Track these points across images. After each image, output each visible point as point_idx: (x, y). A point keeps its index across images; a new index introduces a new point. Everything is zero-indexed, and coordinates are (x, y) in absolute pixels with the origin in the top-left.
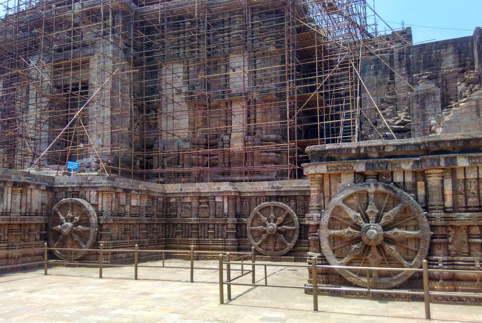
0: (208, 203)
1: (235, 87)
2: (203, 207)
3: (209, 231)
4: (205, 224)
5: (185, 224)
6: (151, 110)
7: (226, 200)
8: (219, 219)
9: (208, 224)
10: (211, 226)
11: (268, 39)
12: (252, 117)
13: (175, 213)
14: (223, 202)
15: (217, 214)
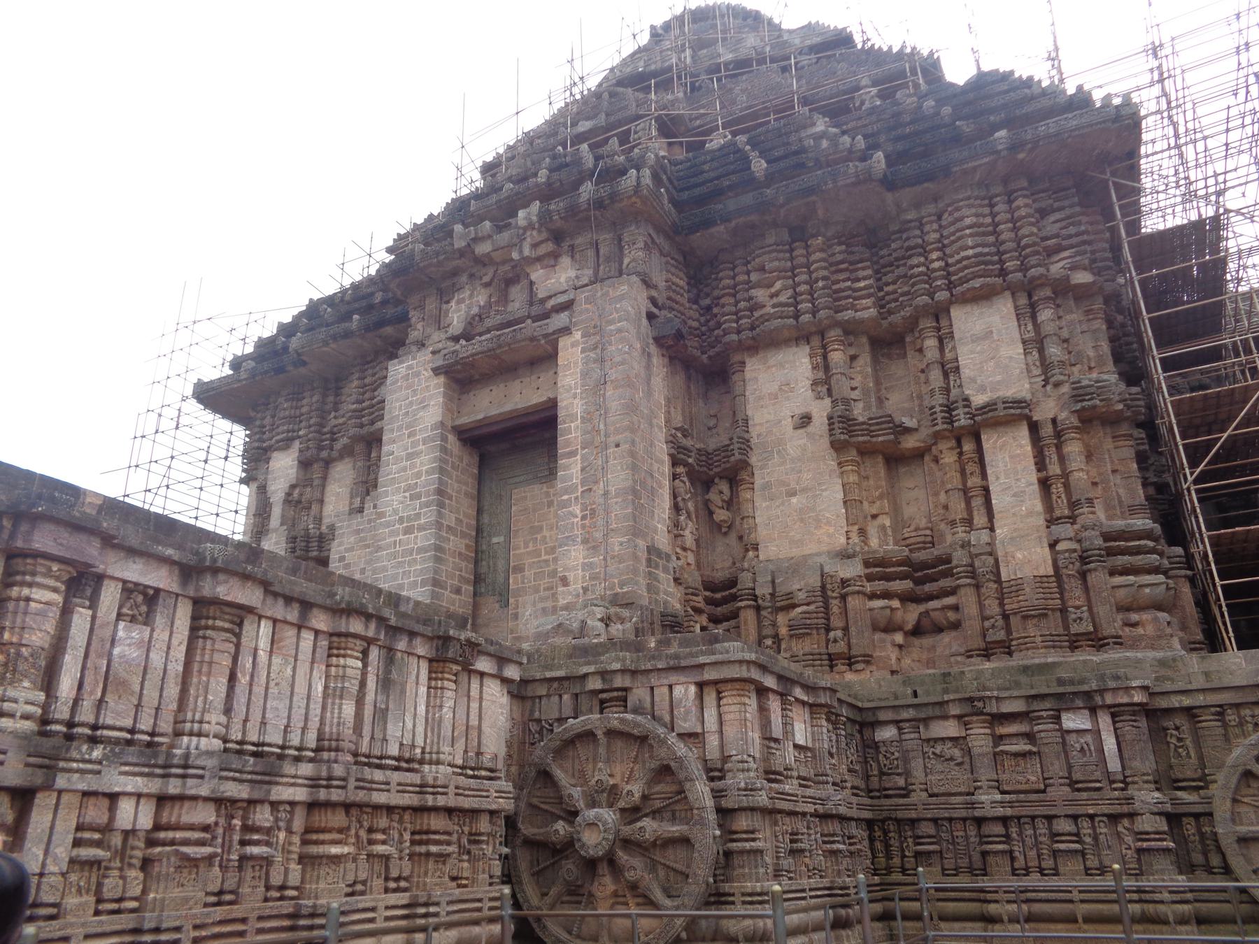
0: (1030, 737)
1: (982, 389)
2: (1016, 755)
3: (1062, 846)
4: (1033, 818)
5: (950, 820)
6: (717, 480)
7: (1105, 721)
8: (1095, 795)
9: (1050, 818)
10: (1064, 826)
11: (1066, 254)
12: (1054, 469)
13: (901, 782)
14: (1097, 733)
15: (1076, 776)
